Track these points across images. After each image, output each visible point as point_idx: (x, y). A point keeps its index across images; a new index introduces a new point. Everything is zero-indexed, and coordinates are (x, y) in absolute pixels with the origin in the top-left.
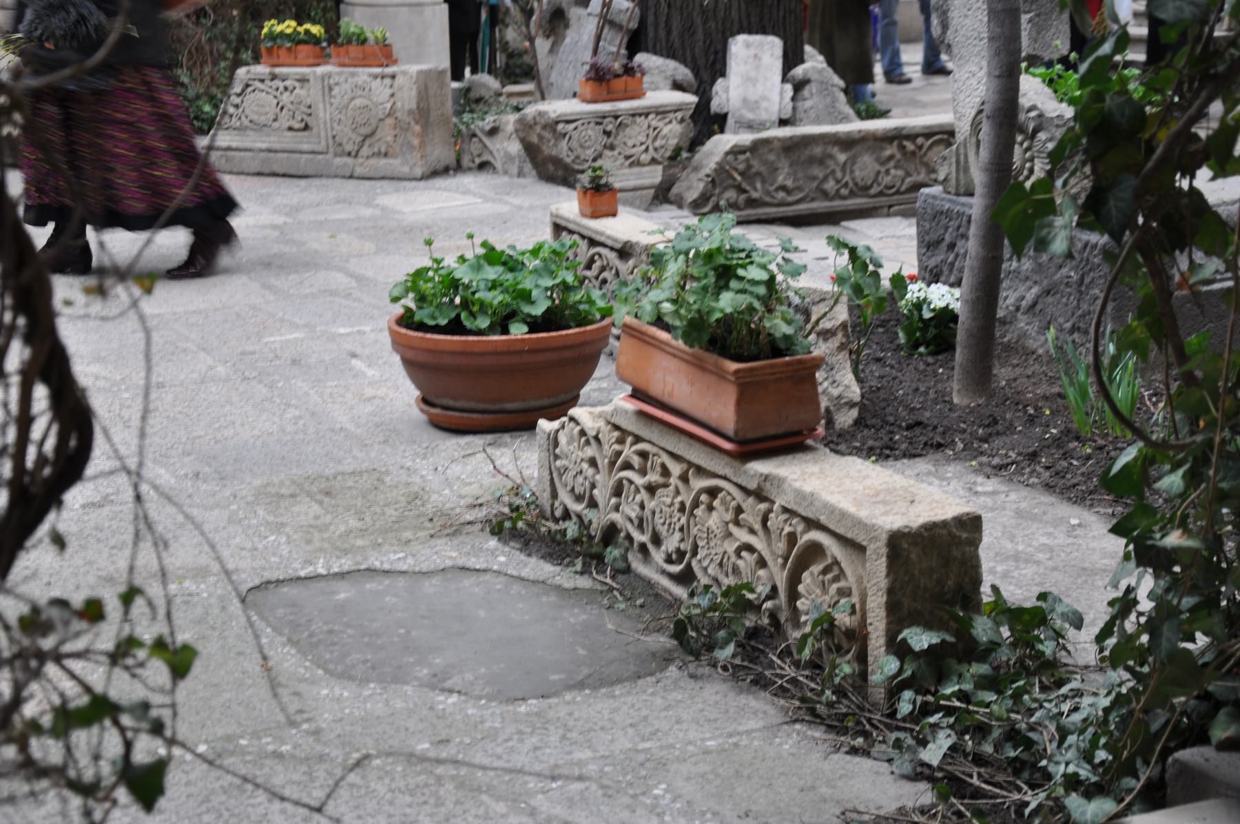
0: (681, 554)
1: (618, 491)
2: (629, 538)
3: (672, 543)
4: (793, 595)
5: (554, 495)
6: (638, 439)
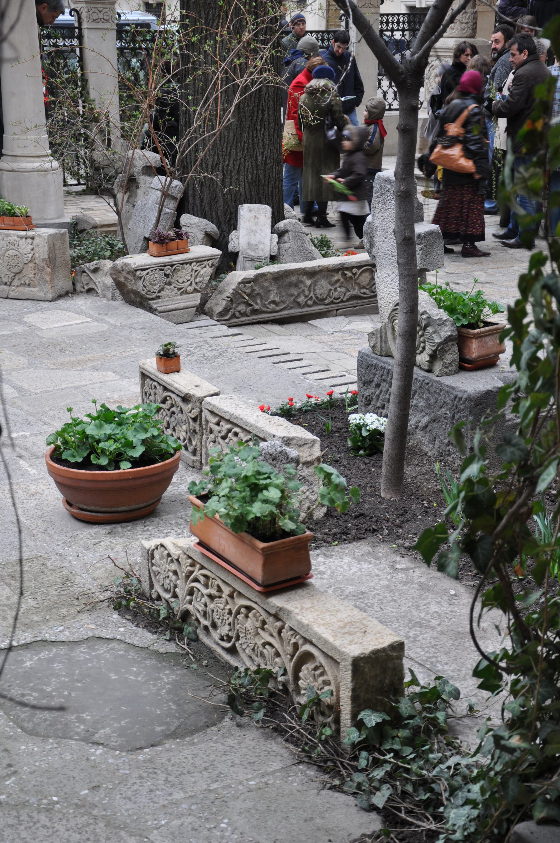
1: (191, 592)
3: (224, 630)
4: (297, 678)
5: (152, 586)
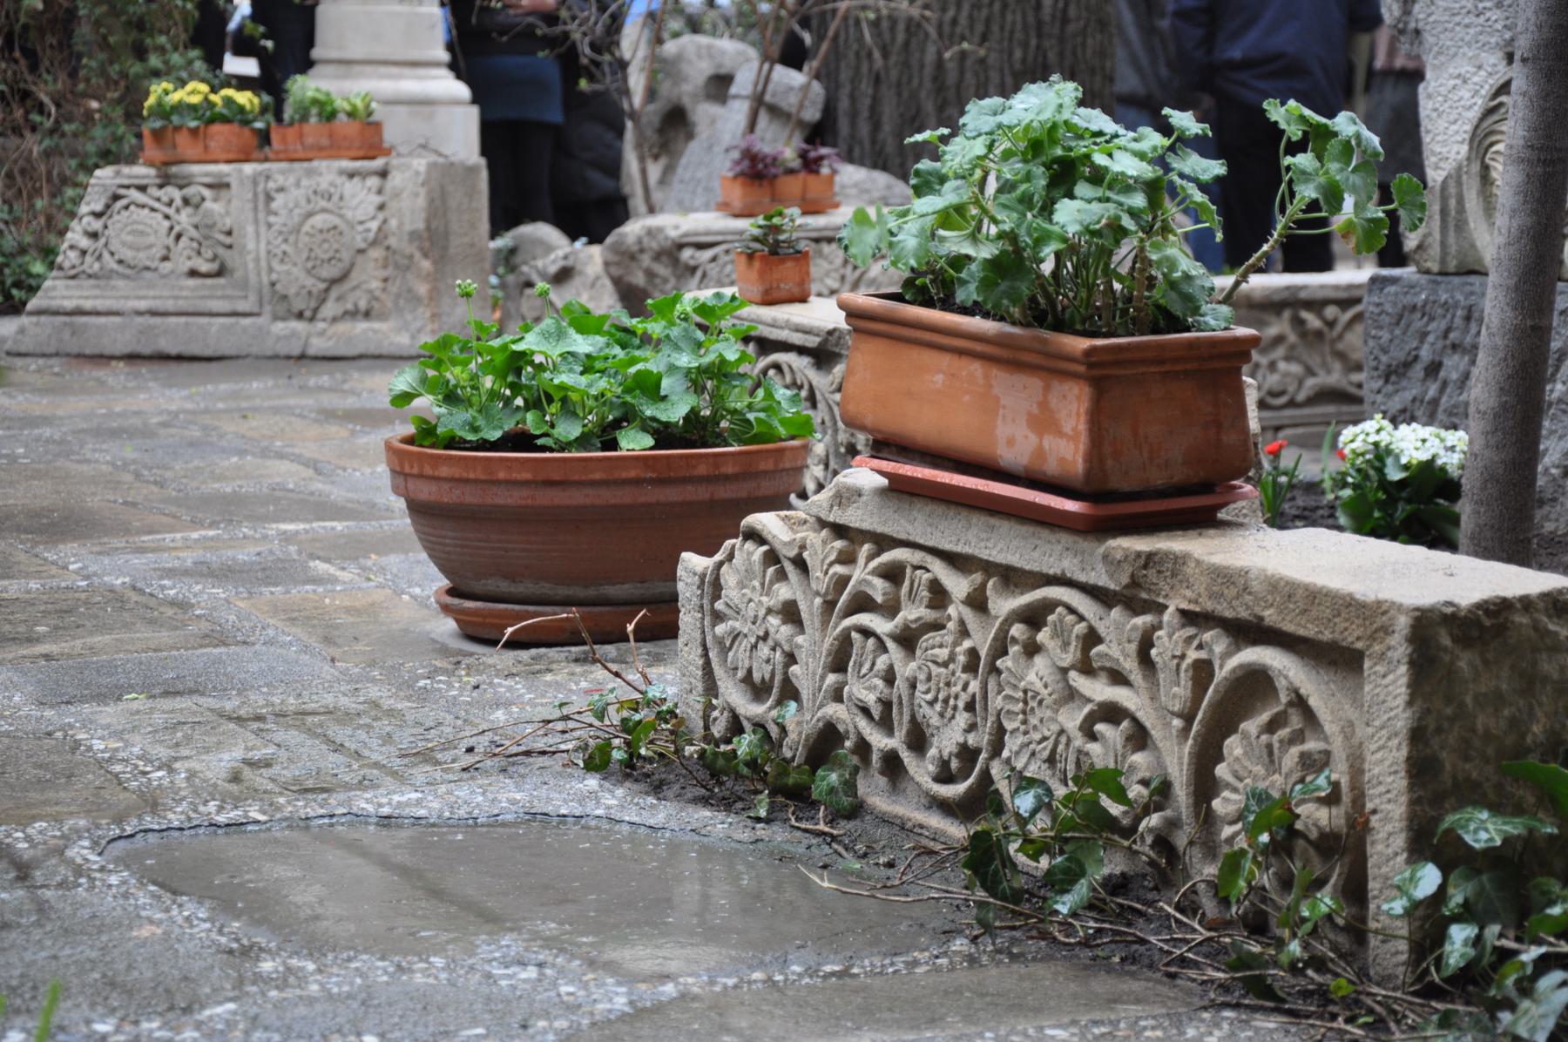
0: (968, 754)
2: (863, 747)
6: (884, 543)
